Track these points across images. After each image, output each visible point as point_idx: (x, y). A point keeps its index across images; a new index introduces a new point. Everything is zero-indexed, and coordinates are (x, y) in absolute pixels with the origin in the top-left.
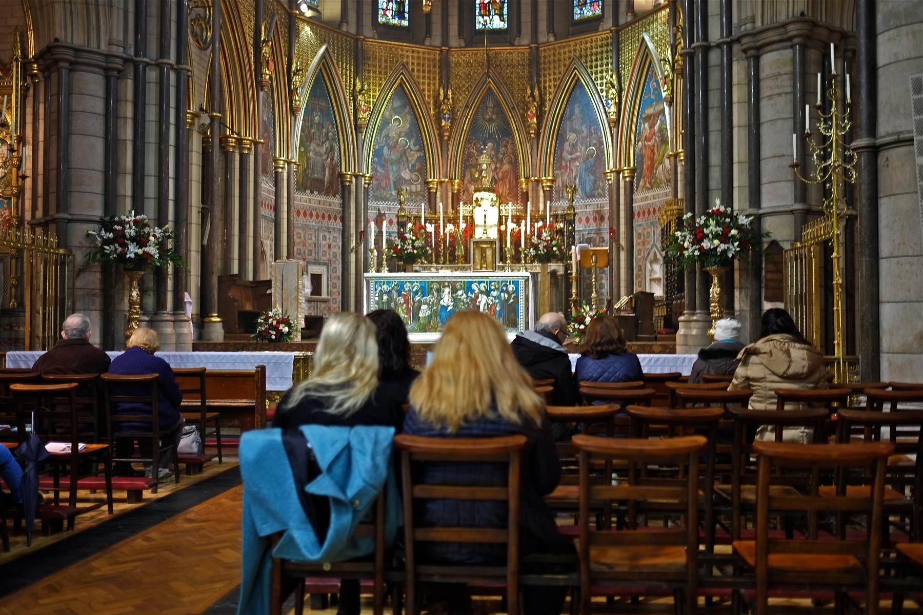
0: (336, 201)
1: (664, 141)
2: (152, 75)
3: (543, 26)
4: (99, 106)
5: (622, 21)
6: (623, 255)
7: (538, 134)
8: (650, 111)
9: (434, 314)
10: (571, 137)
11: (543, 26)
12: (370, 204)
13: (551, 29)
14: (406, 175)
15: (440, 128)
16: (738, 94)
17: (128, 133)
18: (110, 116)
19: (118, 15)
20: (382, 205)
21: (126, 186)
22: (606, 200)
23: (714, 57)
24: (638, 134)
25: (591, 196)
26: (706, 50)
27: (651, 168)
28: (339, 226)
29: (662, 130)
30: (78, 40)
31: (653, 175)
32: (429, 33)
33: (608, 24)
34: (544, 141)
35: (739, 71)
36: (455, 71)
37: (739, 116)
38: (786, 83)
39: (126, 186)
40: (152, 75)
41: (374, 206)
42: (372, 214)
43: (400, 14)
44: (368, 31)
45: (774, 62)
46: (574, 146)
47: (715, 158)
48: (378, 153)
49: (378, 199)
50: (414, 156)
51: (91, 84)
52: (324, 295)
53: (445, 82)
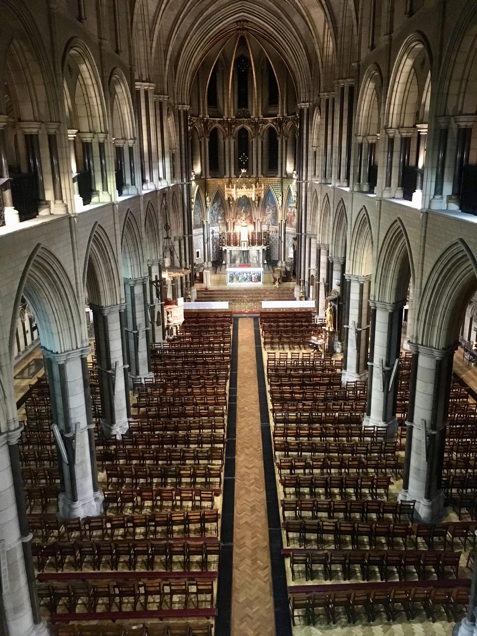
0: (202, 229)
1: (294, 215)
2: (187, 238)
3: (260, 172)
5: (284, 176)
6: (283, 244)
7: (258, 206)
8: (291, 205)
9: (242, 279)
10: (268, 207)
11: (260, 172)
12: (211, 228)
13: (262, 174)
14: (220, 218)
15: (229, 204)
16: (307, 245)
17: (183, 251)
20: (214, 228)
22: (278, 227)
23: (303, 236)
24: (287, 210)
25: (273, 225)
27: (291, 221)
28: (202, 236)
29: (294, 212)
31: (291, 224)
32: (225, 174)
34: (260, 207)
40: (187, 238)
41: (211, 229)
42: (211, 231)
46: (269, 210)
48: (212, 213)
49: (212, 226)
50: (222, 212)
52: (200, 257)
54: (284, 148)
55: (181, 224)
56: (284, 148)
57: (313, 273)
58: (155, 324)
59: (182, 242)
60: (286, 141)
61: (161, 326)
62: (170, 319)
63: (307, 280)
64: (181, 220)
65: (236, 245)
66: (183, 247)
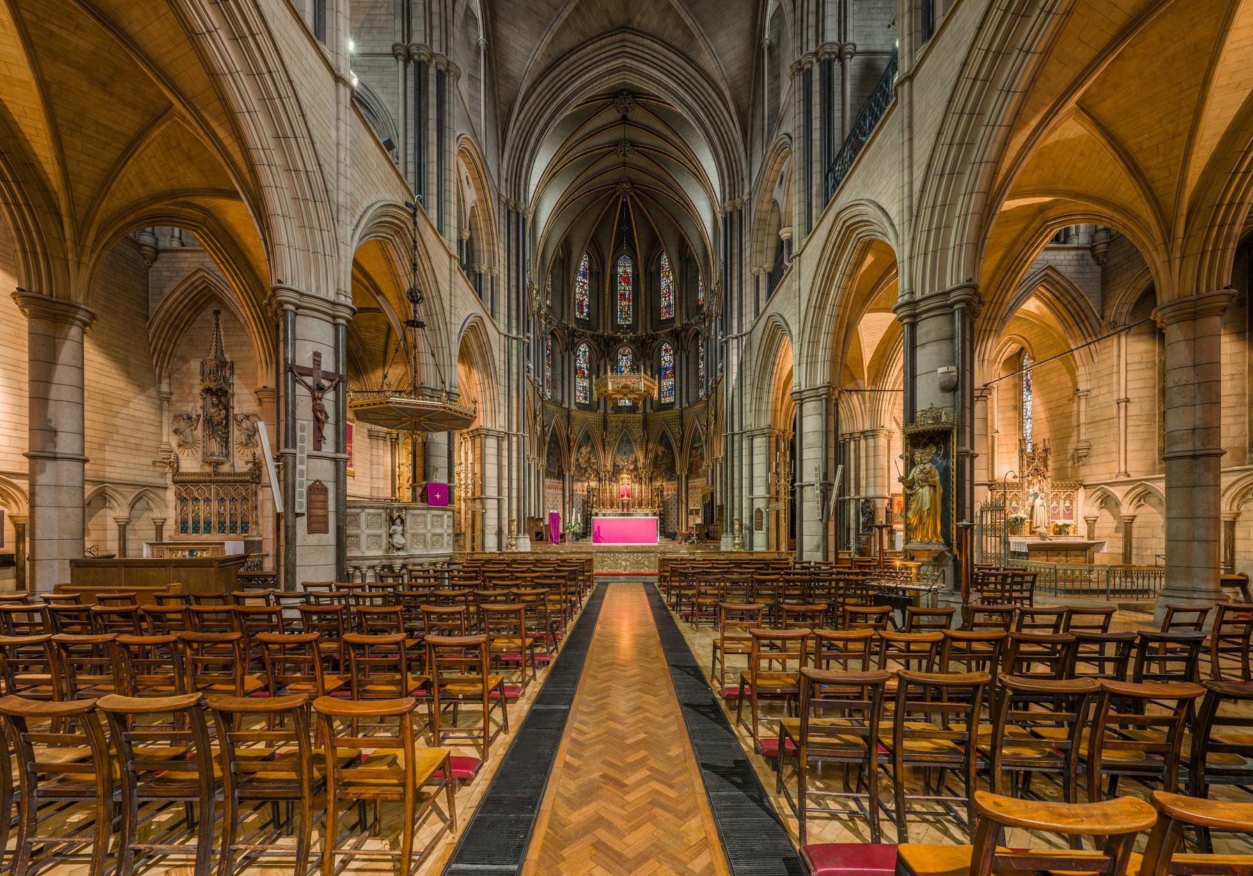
2: (514, 439)
4: (495, 451)
17: (505, 462)
18: (499, 455)
19: (502, 415)
21: (505, 484)
23: (736, 438)
26: (733, 435)
28: (560, 492)
30: (489, 426)
33: (677, 406)
35: (745, 444)
36: (610, 424)
37: (745, 460)
38: (763, 450)
39: (505, 484)
40: (514, 439)
43: (585, 398)
44: (573, 407)
45: (759, 442)
47: (736, 476)
51: (491, 443)
53: (605, 428)
54: (684, 367)
55: (504, 409)
56: (684, 367)
57: (759, 504)
58: (302, 523)
59: (505, 444)
60: (687, 357)
61: (330, 538)
62: (398, 539)
63: (746, 521)
64: (503, 400)
65: (612, 505)
66: (505, 453)
